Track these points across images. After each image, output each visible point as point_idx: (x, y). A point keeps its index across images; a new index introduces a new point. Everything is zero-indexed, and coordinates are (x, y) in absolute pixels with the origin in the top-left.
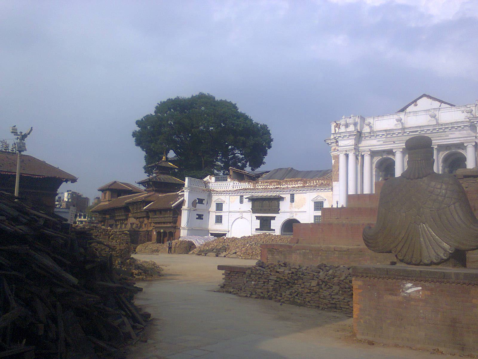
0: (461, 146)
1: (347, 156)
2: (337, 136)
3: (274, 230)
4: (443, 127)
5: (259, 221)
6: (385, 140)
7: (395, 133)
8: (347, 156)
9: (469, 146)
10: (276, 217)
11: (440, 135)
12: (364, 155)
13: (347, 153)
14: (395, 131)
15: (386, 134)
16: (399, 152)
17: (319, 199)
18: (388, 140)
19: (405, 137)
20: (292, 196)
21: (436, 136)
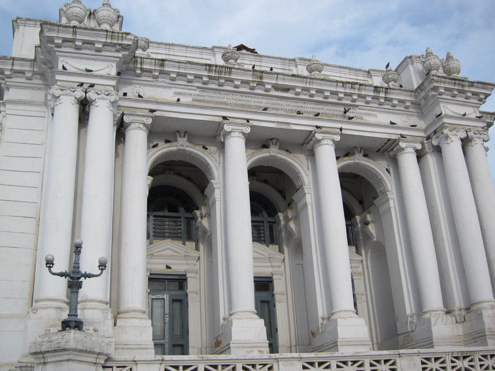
0: (388, 150)
1: (84, 106)
2: (61, 35)
4: (356, 92)
7: (232, 81)
8: (84, 106)
14: (238, 74)
15: (208, 76)
16: (241, 135)
18: (207, 96)
19: (256, 100)
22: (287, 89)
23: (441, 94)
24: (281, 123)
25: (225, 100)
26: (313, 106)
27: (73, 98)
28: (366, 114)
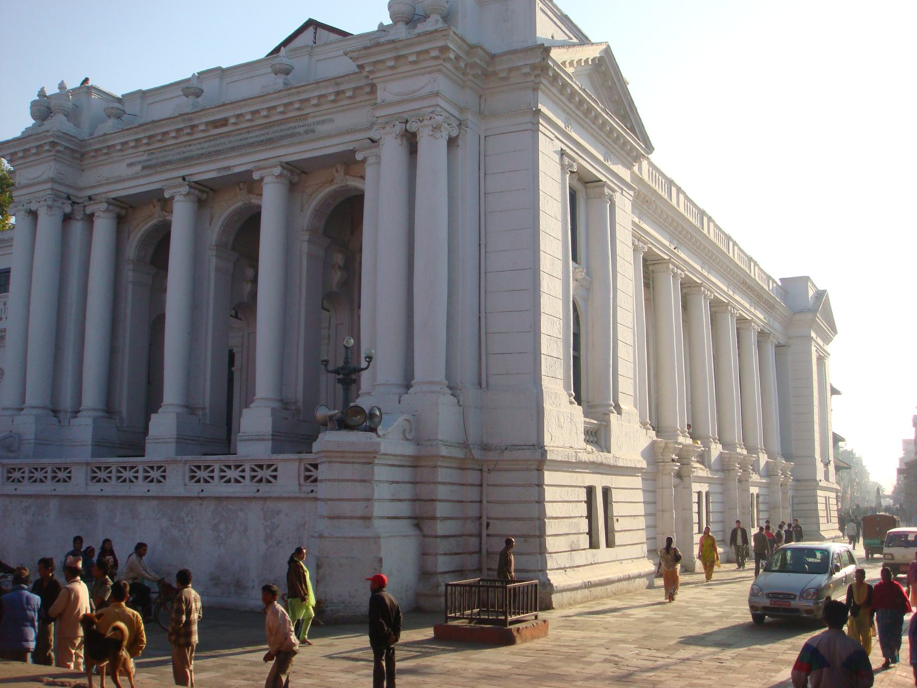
6: (147, 161)
9: (371, 160)
11: (293, 131)
12: (92, 215)
13: (33, 207)
16: (182, 198)
19: (199, 146)
21: (282, 134)
22: (224, 122)
23: (371, 72)
24: (221, 169)
25: (170, 158)
26: (257, 133)
27: (23, 213)
28: (319, 123)
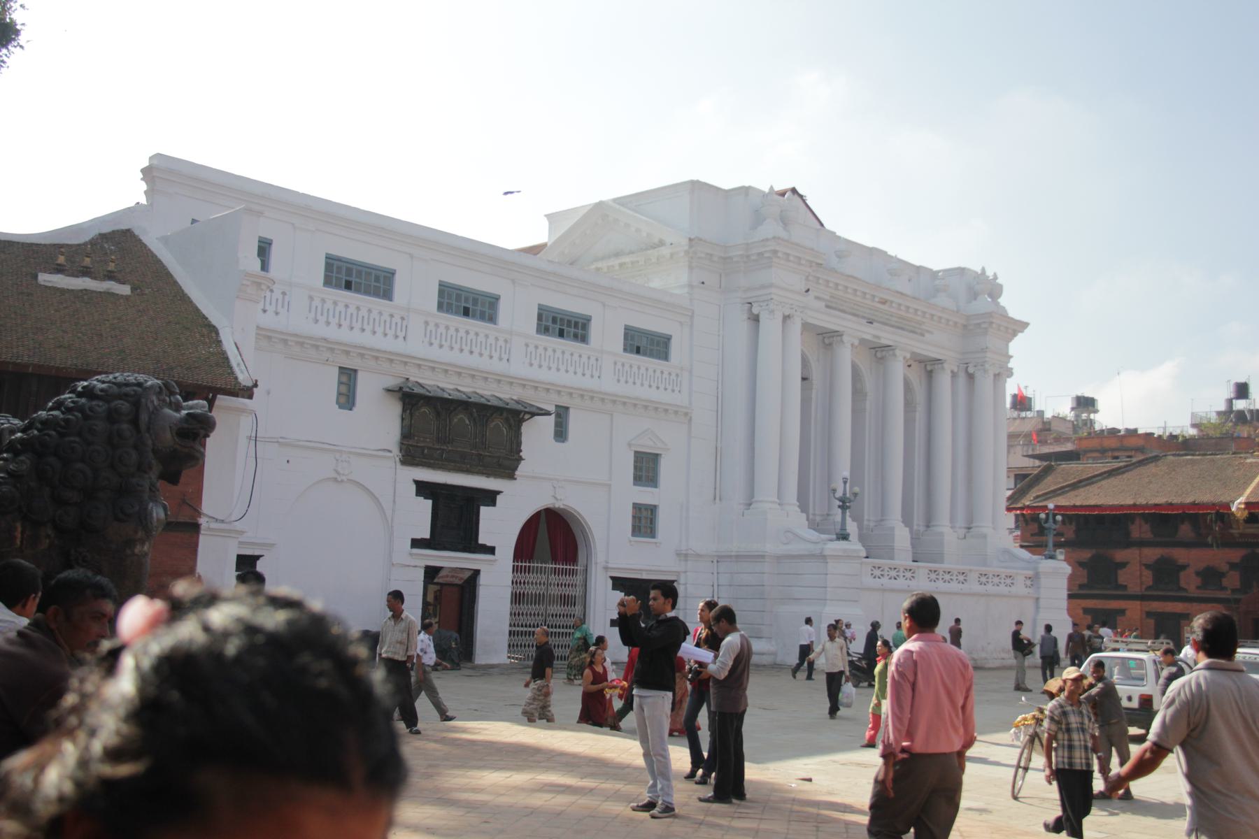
3: (491, 550)
5: (430, 502)
10: (499, 493)
17: (648, 446)
20: (562, 415)
